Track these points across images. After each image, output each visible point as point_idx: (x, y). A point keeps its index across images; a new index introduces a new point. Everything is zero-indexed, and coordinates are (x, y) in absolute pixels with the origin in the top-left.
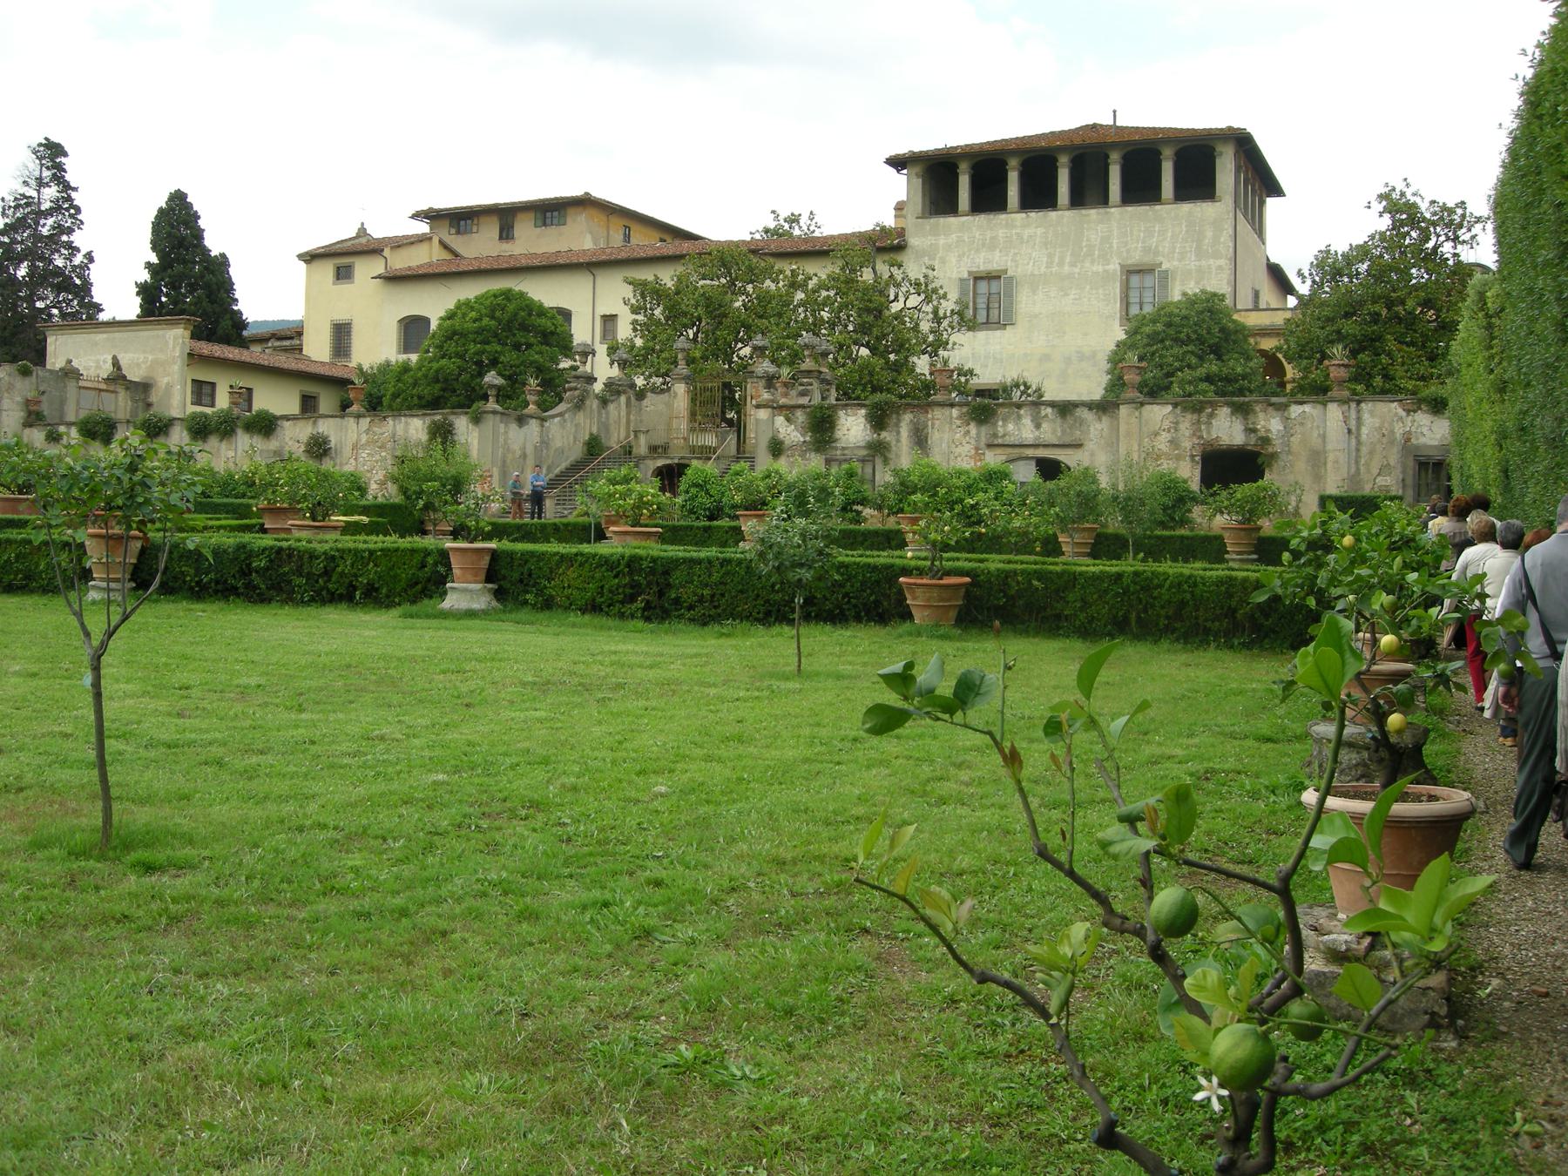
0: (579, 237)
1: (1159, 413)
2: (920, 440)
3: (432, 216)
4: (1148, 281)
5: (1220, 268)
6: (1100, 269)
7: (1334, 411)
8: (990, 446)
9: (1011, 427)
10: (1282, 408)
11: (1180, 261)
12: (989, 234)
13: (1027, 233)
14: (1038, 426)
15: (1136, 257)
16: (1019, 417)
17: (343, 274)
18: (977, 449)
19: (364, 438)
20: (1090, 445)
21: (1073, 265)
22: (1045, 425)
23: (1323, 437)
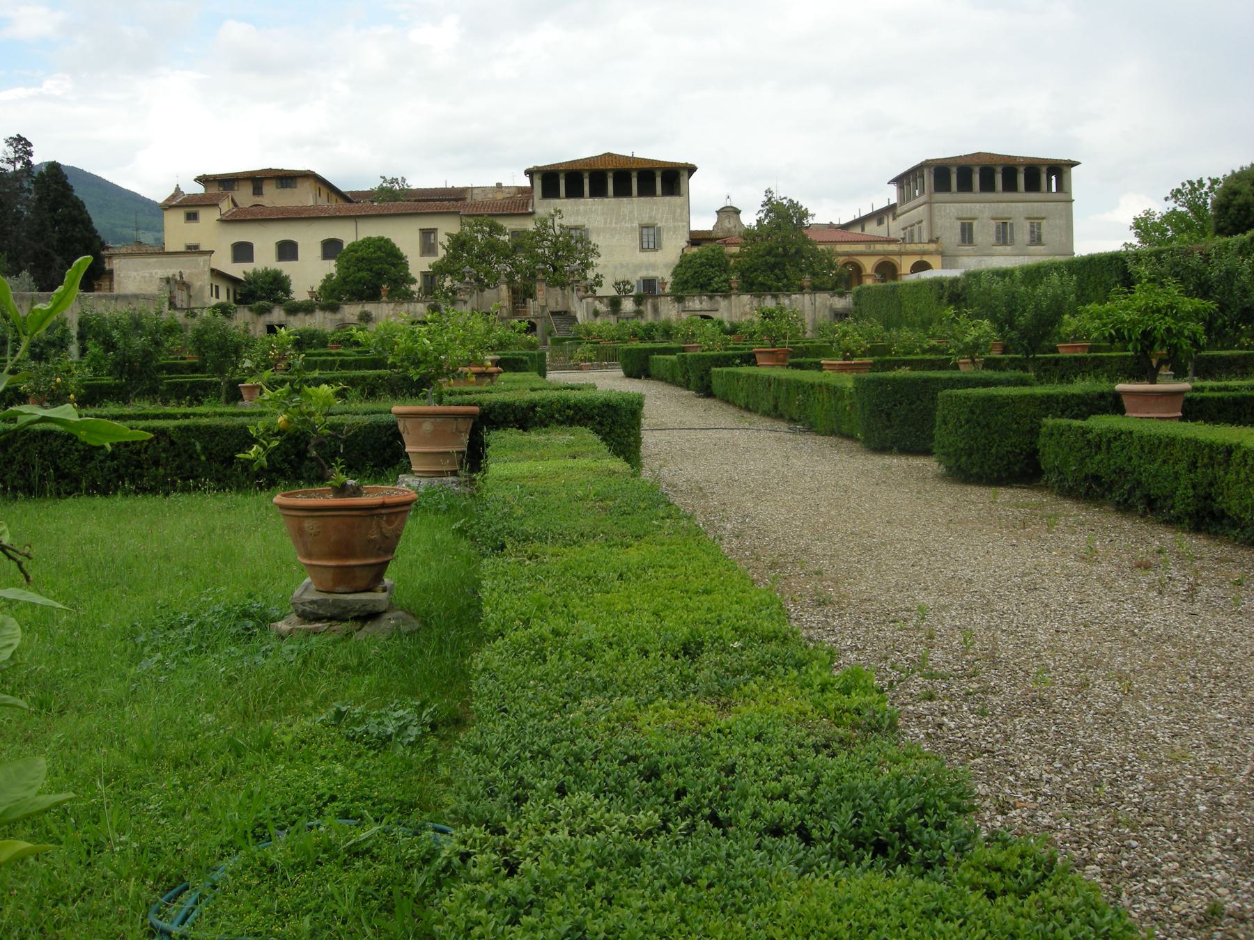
0: (304, 197)
1: (746, 298)
2: (656, 310)
3: (204, 180)
4: (651, 231)
7: (807, 296)
8: (683, 311)
10: (789, 296)
15: (646, 221)
17: (192, 217)
19: (391, 313)
20: (721, 310)
21: (616, 223)
23: (803, 306)
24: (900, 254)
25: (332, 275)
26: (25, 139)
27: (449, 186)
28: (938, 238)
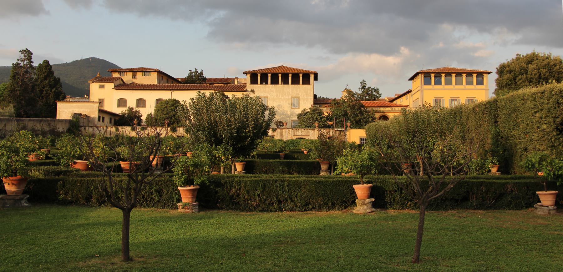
5: (311, 98)
6: (287, 97)
8: (294, 136)
9: (297, 133)
11: (303, 96)
12: (264, 89)
13: (272, 89)
15: (294, 95)
22: (303, 132)
24: (389, 112)
25: (151, 114)
26: (30, 51)
27: (226, 77)
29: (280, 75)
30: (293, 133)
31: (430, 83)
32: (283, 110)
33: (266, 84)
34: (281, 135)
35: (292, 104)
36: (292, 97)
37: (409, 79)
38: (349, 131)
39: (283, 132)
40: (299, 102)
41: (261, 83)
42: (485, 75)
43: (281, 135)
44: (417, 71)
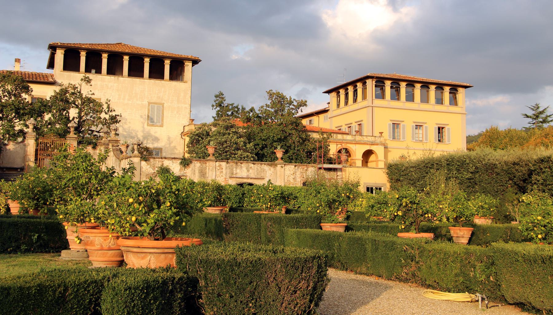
8: (230, 177)
9: (238, 171)
14: (248, 171)
15: (154, 100)
16: (241, 167)
18: (225, 178)
22: (251, 171)
28: (381, 133)
29: (126, 59)
30: (228, 170)
31: (383, 96)
32: (129, 127)
33: (96, 72)
34: (203, 173)
35: (148, 116)
36: (149, 103)
37: (324, 91)
38: (345, 171)
39: (206, 168)
40: (163, 114)
41: (88, 70)
42: (460, 90)
43: (203, 173)
44: (365, 75)
